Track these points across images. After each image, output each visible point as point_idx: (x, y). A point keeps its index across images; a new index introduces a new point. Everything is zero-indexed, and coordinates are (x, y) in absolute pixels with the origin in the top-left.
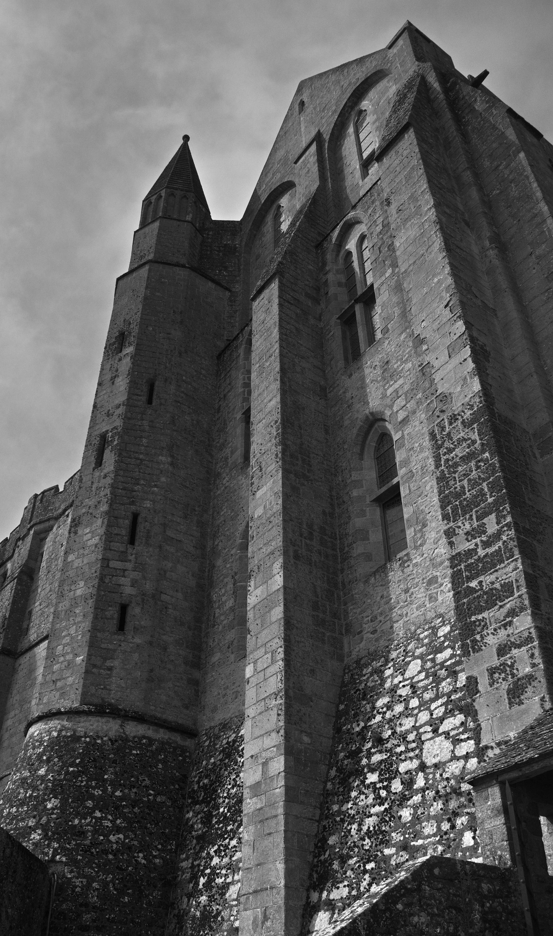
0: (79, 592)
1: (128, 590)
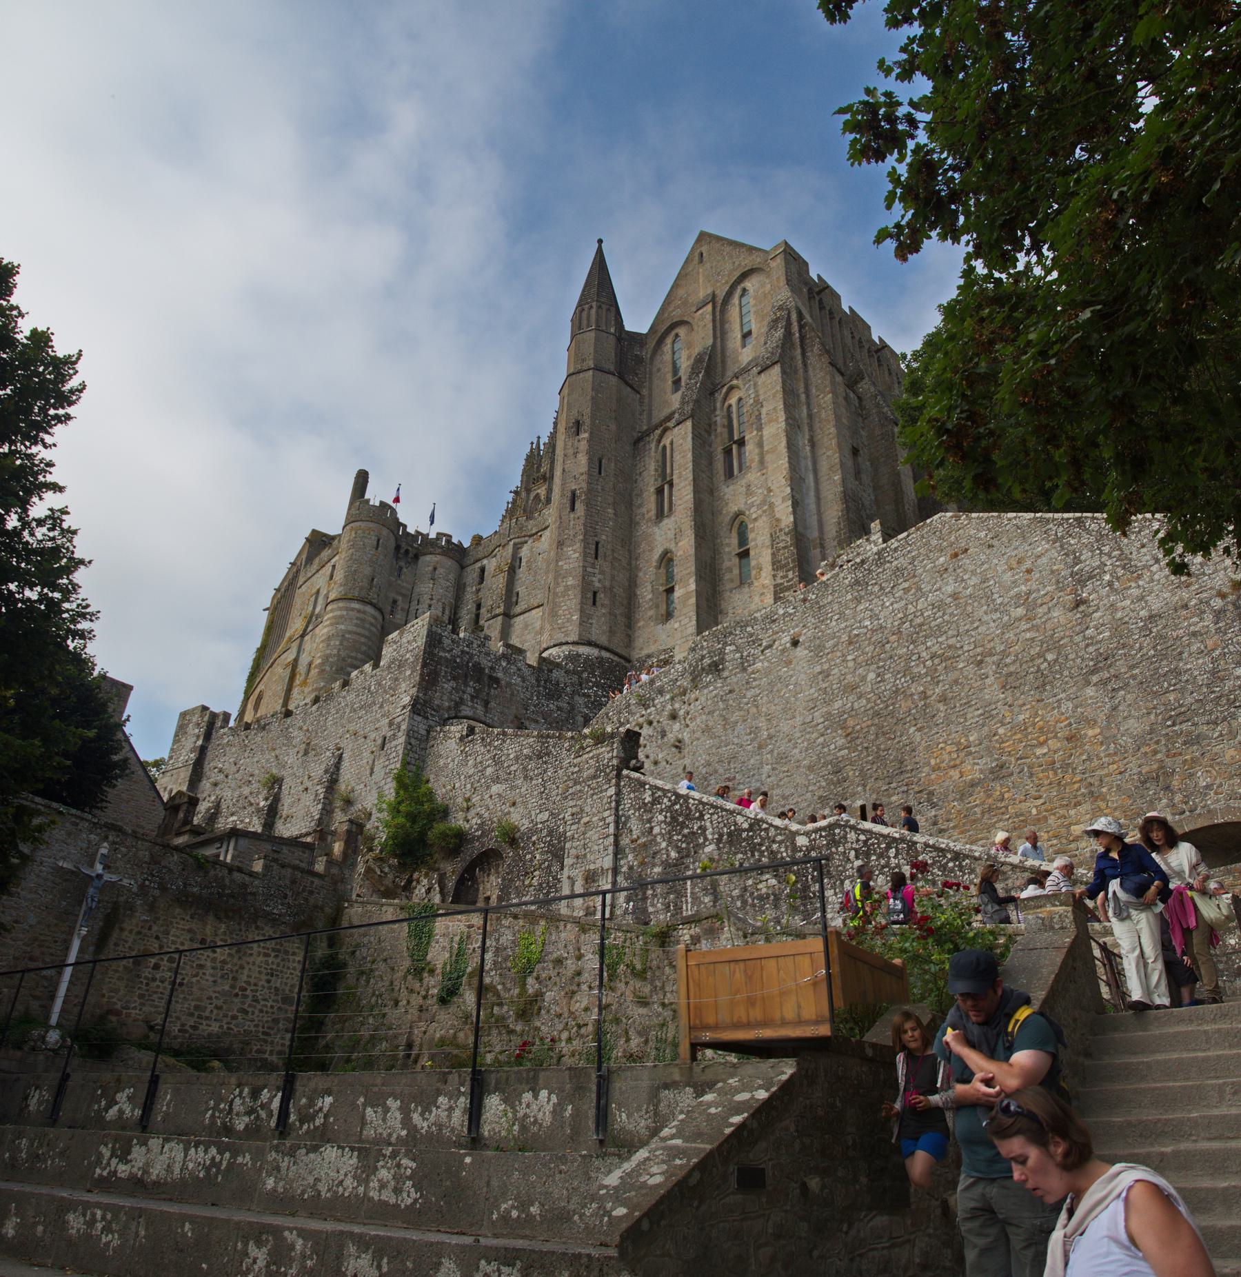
0: (569, 583)
1: (597, 584)
